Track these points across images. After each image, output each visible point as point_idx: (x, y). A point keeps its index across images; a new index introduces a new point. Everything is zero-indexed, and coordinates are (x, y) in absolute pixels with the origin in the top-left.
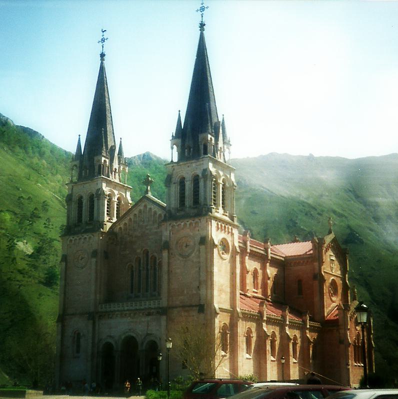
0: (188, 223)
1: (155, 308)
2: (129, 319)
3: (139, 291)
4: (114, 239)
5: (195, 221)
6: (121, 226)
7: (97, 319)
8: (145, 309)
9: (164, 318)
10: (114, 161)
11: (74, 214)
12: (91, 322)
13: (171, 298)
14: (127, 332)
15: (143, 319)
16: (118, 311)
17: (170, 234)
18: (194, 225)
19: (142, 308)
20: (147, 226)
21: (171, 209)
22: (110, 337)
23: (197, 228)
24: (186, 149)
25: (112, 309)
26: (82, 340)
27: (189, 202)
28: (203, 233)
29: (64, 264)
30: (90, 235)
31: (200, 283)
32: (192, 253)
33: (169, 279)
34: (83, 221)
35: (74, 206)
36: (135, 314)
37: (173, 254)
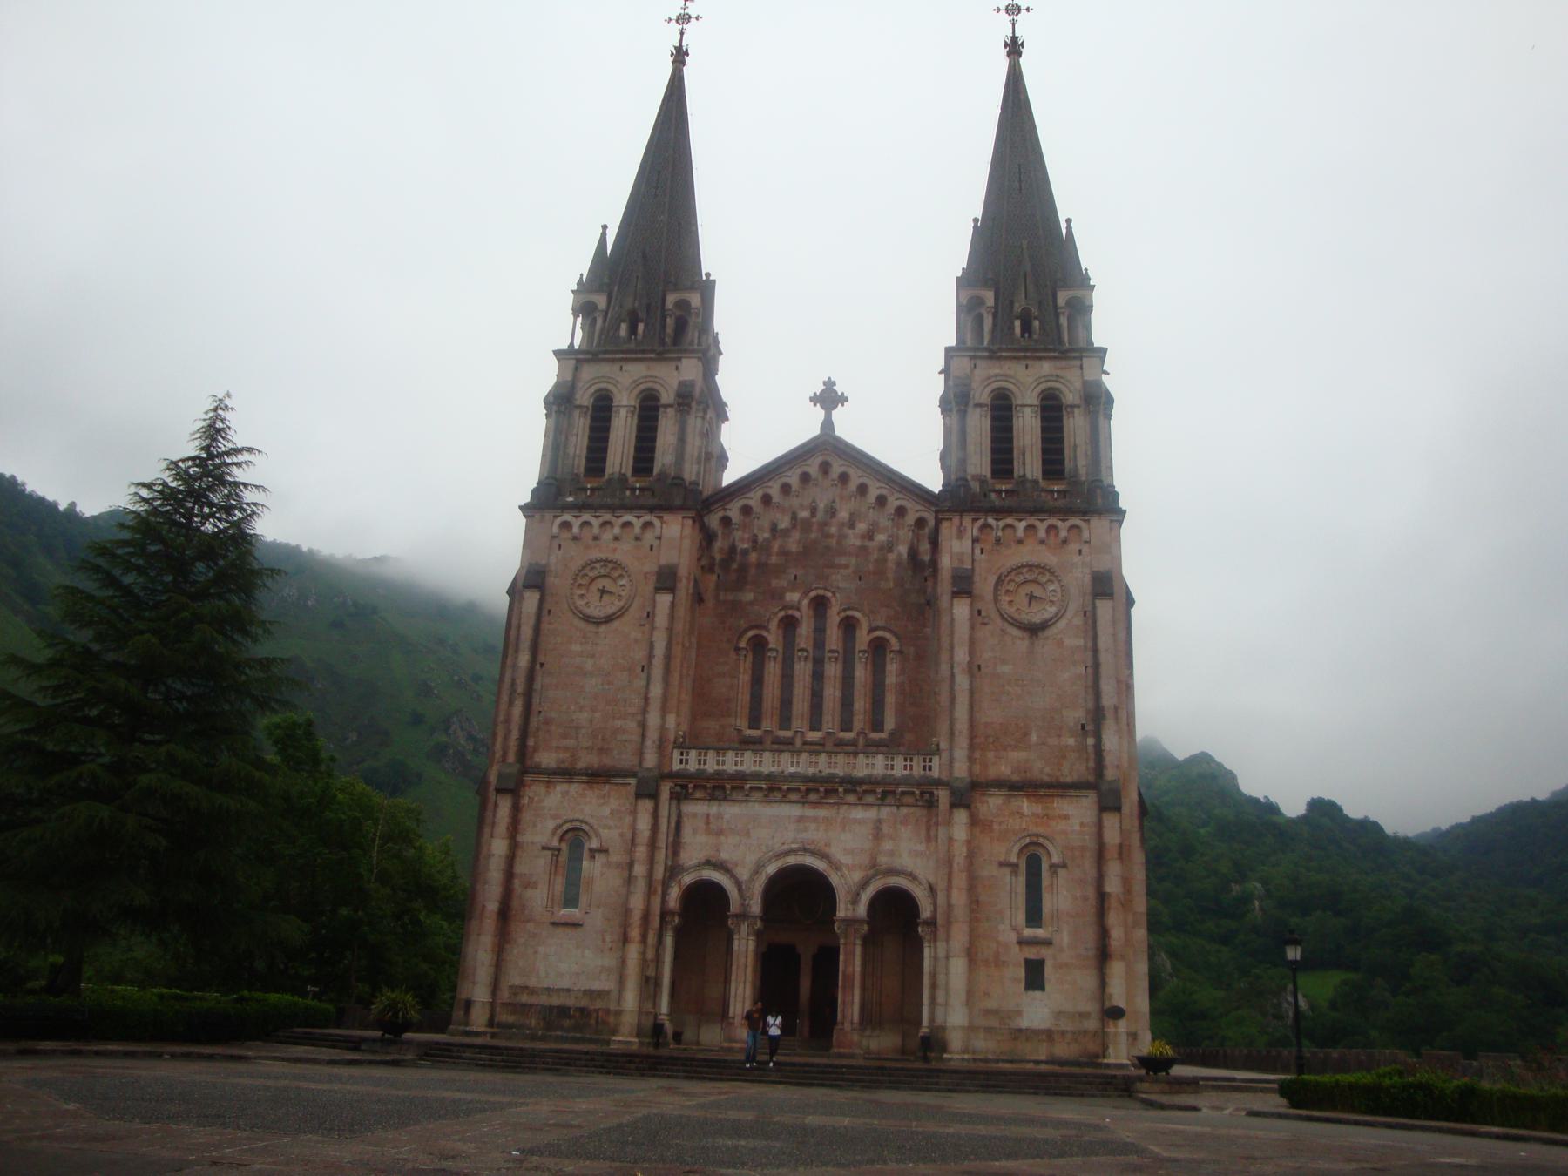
1: (906, 780)
2: (795, 811)
3: (785, 722)
5: (1068, 523)
6: (729, 513)
9: (961, 816)
11: (579, 444)
13: (977, 754)
15: (858, 813)
17: (973, 549)
20: (824, 524)
21: (969, 478)
22: (721, 866)
23: (1074, 547)
27: (1030, 464)
28: (1102, 565)
29: (531, 600)
30: (648, 518)
32: (1057, 617)
36: (828, 792)
37: (983, 614)
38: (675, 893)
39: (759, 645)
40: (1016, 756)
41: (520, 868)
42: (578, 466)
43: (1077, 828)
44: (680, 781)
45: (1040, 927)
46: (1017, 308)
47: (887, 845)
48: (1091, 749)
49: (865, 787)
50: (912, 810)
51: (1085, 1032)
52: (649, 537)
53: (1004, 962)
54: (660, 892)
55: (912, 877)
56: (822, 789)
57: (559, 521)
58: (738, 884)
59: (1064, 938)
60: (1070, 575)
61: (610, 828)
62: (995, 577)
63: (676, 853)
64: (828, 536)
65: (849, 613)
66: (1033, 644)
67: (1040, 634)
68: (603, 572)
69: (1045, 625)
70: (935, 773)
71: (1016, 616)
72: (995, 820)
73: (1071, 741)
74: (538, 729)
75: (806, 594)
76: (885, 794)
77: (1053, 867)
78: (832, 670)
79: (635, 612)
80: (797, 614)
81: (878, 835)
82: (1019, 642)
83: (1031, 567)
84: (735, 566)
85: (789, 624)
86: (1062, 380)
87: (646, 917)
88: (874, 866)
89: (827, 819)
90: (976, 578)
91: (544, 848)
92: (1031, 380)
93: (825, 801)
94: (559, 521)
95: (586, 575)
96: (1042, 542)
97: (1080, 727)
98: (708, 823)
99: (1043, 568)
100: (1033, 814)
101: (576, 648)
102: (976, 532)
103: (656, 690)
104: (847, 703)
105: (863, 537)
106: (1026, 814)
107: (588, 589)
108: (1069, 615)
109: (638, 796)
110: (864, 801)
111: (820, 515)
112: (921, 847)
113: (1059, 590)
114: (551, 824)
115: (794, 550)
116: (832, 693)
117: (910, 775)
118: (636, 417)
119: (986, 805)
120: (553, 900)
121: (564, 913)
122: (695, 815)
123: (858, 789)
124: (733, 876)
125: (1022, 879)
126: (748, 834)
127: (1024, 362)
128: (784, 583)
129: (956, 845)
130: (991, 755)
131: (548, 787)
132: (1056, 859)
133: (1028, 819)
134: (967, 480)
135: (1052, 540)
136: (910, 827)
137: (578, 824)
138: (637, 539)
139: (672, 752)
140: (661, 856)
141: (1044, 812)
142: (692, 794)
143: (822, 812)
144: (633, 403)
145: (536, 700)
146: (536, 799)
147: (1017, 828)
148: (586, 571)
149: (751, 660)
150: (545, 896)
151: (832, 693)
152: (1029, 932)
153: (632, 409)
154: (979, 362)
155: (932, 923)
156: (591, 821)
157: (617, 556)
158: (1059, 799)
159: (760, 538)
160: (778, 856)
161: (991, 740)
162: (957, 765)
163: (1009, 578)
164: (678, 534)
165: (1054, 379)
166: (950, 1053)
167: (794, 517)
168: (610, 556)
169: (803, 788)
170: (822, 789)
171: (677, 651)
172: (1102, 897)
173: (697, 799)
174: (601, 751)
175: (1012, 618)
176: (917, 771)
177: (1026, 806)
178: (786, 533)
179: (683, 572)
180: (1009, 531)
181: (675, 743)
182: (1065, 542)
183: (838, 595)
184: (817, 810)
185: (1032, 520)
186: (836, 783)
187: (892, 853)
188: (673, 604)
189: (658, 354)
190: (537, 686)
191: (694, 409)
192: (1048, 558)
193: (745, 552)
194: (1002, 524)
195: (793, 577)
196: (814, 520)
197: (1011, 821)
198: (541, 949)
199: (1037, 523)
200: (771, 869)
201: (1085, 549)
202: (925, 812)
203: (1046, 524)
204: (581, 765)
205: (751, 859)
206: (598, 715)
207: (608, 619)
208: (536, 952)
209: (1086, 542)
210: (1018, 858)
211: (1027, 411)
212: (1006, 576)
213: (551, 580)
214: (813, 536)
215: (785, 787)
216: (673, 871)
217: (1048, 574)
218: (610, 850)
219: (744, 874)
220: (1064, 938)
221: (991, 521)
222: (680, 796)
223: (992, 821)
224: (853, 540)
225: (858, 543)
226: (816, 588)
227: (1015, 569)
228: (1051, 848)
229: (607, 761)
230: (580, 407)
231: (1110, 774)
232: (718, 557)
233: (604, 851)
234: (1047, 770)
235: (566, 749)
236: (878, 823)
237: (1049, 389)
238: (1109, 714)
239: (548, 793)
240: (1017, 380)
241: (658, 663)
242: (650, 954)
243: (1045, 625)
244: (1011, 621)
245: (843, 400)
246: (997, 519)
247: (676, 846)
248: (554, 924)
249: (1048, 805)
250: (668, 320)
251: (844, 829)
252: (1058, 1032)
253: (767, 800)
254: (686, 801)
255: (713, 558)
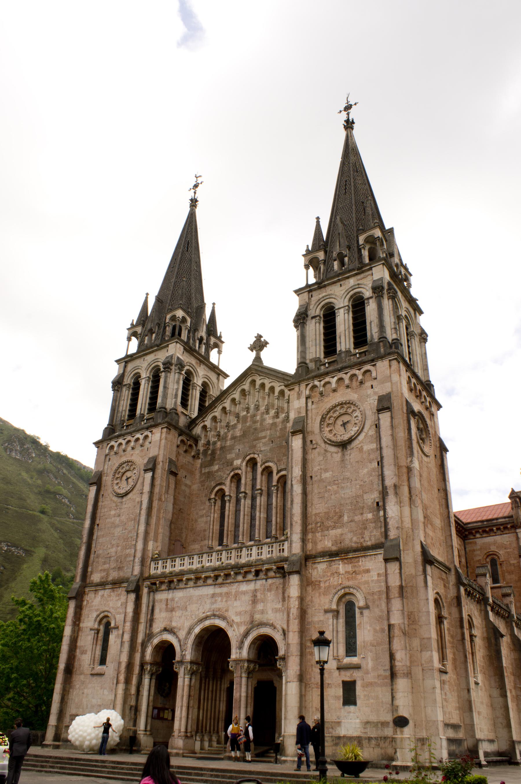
0: (346, 378)
1: (269, 561)
2: (209, 590)
4: (190, 446)
5: (362, 370)
6: (206, 423)
7: (145, 590)
8: (249, 565)
10: (202, 325)
12: (132, 596)
13: (310, 536)
14: (206, 618)
15: (244, 587)
16: (190, 572)
17: (307, 403)
18: (360, 377)
19: (243, 560)
20: (254, 415)
21: (308, 361)
23: (368, 384)
24: (335, 260)
25: (178, 569)
26: (113, 638)
30: (147, 433)
31: (384, 493)
32: (359, 433)
33: (305, 493)
34: (138, 412)
35: (126, 394)
36: (227, 576)
37: (314, 442)
38: (149, 650)
39: (221, 494)
40: (333, 533)
41: (79, 644)
42: (124, 416)
43: (375, 578)
44: (153, 581)
45: (356, 656)
46: (335, 254)
47: (260, 607)
48: (382, 519)
49: (245, 569)
50: (274, 580)
51: (385, 738)
52: (147, 443)
53: (328, 684)
54: (140, 651)
55: (273, 626)
56: (222, 574)
57: (109, 446)
58: (179, 641)
59: (369, 664)
60: (366, 403)
61: (120, 614)
62: (321, 417)
63: (151, 626)
64: (255, 422)
65: (267, 464)
66: (343, 455)
67: (349, 447)
68: (127, 468)
69: (351, 440)
70: (286, 554)
71: (334, 439)
72: (322, 580)
73: (370, 516)
74: (93, 562)
75: (244, 459)
76: (257, 573)
77: (360, 608)
78: (261, 501)
79: (138, 486)
80: (239, 472)
81: (254, 601)
82: (335, 455)
83: (341, 404)
84: (210, 452)
85: (237, 478)
86: (362, 286)
87: (130, 666)
88: (252, 622)
89: (227, 593)
90: (309, 421)
91: (91, 629)
92: (343, 292)
93: (225, 582)
94: (109, 446)
95: (120, 472)
96: (348, 387)
97: (375, 505)
98: (167, 605)
99: (349, 403)
100: (346, 572)
101: (113, 512)
102: (308, 392)
103: (142, 528)
104: (268, 521)
105: (274, 417)
106: (341, 573)
107: (121, 480)
108: (365, 430)
109: (128, 592)
110: (246, 579)
111: (251, 411)
112: (279, 606)
113: (359, 415)
114: (95, 615)
115: (238, 435)
116: (260, 515)
117: (272, 557)
118: (150, 383)
119: (316, 570)
120: (94, 660)
121: (99, 669)
122: (161, 601)
123: (241, 571)
124: (177, 637)
125: (342, 621)
126: (186, 608)
127: (339, 284)
128: (233, 455)
129: (292, 600)
130: (318, 535)
131: (95, 594)
132: (362, 603)
133: (343, 576)
134: (306, 364)
135: (355, 384)
136: (273, 592)
137: (106, 613)
138: (142, 446)
139: (150, 564)
140: (142, 628)
141: (354, 570)
142: (160, 587)
143: (224, 590)
144: (148, 375)
145: (93, 546)
146: (90, 601)
147: (336, 583)
148: (120, 470)
149: (220, 505)
150: (90, 658)
151: (260, 515)
152: (347, 660)
153: (147, 378)
154: (314, 293)
155: (283, 659)
156: (112, 610)
157: (133, 458)
158: (363, 559)
159: (222, 433)
160: (201, 620)
161: (319, 525)
162: (294, 545)
163: (329, 416)
164: (159, 438)
165: (357, 286)
166: (285, 756)
167: (237, 416)
168: (129, 459)
169: (212, 575)
170: (222, 574)
171: (155, 504)
172: (390, 627)
173: (162, 590)
174: (120, 569)
175: (330, 440)
176: (276, 554)
177: (342, 567)
178: (234, 427)
179: (160, 459)
180: (328, 386)
181: (152, 558)
182: (361, 383)
183: (260, 455)
184: (222, 588)
185: (341, 375)
186: (229, 569)
187: (262, 612)
188: (153, 478)
189: (158, 346)
190: (95, 537)
191: (173, 370)
192: (352, 396)
193: (215, 443)
194: (322, 383)
195: (238, 450)
196: (249, 415)
197: (332, 579)
198: (85, 691)
199: (344, 376)
200: (197, 630)
201: (375, 383)
202: (281, 581)
203: (349, 375)
204: (110, 578)
205: (187, 625)
206: (119, 548)
207: (127, 494)
208: (83, 693)
209: (376, 379)
210: (338, 605)
211: (342, 311)
212: (327, 414)
213: (104, 478)
214: (248, 424)
215: (203, 576)
216: (149, 636)
217: (352, 406)
218: (120, 627)
219: (182, 634)
220: (369, 664)
221: (316, 383)
222: (154, 588)
223: (320, 581)
224: (269, 420)
225: (271, 421)
226: (249, 454)
227: (332, 409)
228: (358, 595)
229: (122, 574)
230: (125, 385)
231: (393, 534)
232: (201, 449)
233: (117, 628)
234: (355, 539)
235: (104, 570)
236: (256, 591)
237: (355, 294)
238: (391, 491)
239: (95, 597)
240: (336, 295)
241: (144, 512)
242: (133, 690)
243: (351, 440)
244: (331, 443)
245: (266, 343)
246: (320, 381)
247: (151, 621)
248: (92, 675)
249: (356, 564)
250: (167, 328)
251: (236, 600)
252: (366, 738)
253: (196, 586)
254: (158, 593)
255: (199, 450)
